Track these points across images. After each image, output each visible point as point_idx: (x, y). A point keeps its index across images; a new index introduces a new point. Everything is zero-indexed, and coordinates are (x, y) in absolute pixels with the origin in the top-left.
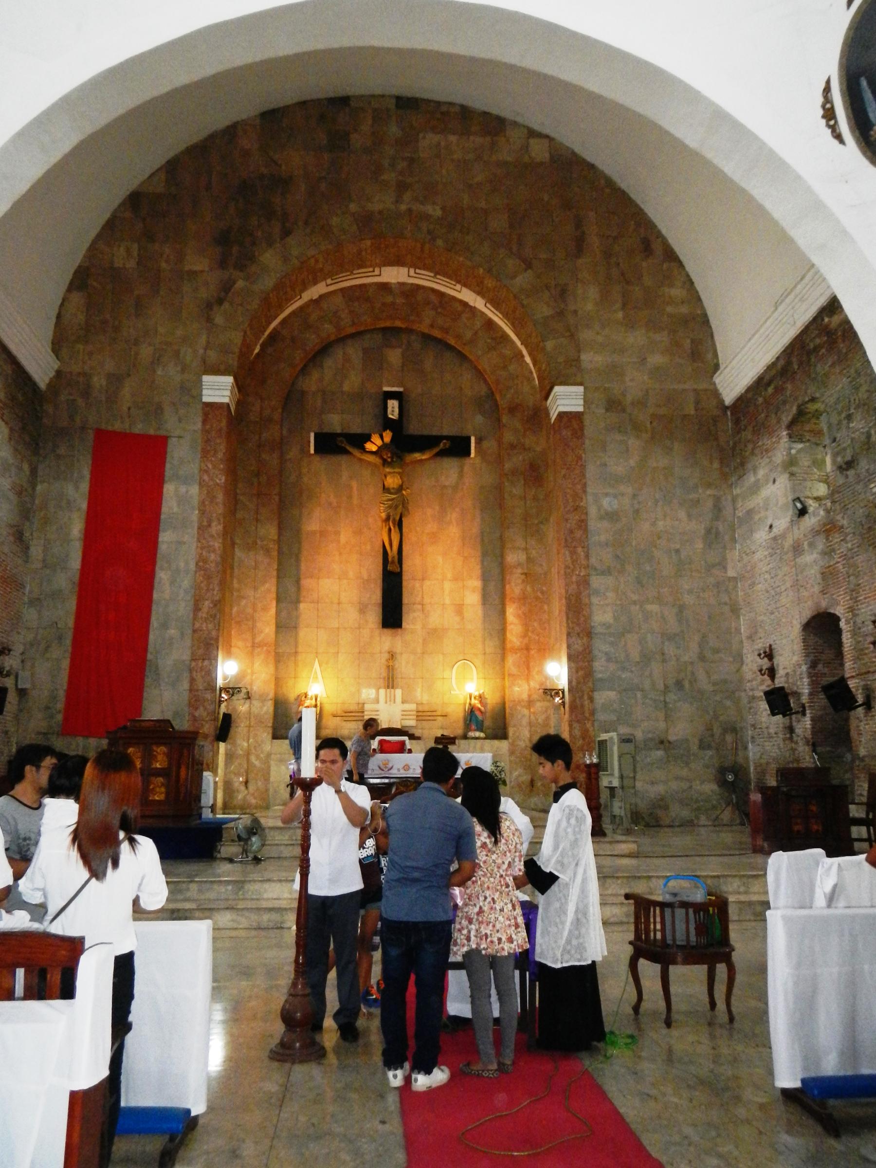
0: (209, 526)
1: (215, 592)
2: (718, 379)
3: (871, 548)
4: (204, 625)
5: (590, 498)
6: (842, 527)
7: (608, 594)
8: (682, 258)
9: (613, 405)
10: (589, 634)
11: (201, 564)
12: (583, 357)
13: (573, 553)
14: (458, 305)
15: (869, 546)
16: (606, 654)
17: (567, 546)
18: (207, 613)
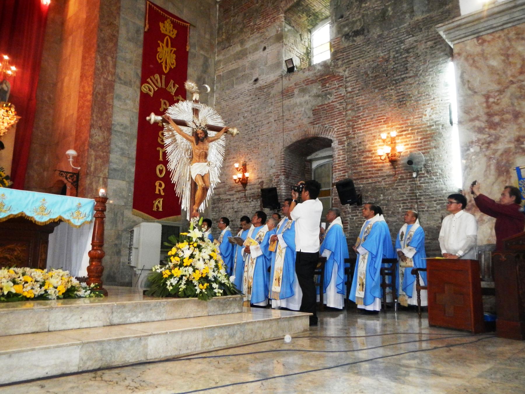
3: (376, 91)
5: (122, 22)
6: (342, 76)
7: (128, 102)
10: (109, 129)
13: (104, 58)
15: (375, 88)
16: (122, 149)
17: (99, 51)
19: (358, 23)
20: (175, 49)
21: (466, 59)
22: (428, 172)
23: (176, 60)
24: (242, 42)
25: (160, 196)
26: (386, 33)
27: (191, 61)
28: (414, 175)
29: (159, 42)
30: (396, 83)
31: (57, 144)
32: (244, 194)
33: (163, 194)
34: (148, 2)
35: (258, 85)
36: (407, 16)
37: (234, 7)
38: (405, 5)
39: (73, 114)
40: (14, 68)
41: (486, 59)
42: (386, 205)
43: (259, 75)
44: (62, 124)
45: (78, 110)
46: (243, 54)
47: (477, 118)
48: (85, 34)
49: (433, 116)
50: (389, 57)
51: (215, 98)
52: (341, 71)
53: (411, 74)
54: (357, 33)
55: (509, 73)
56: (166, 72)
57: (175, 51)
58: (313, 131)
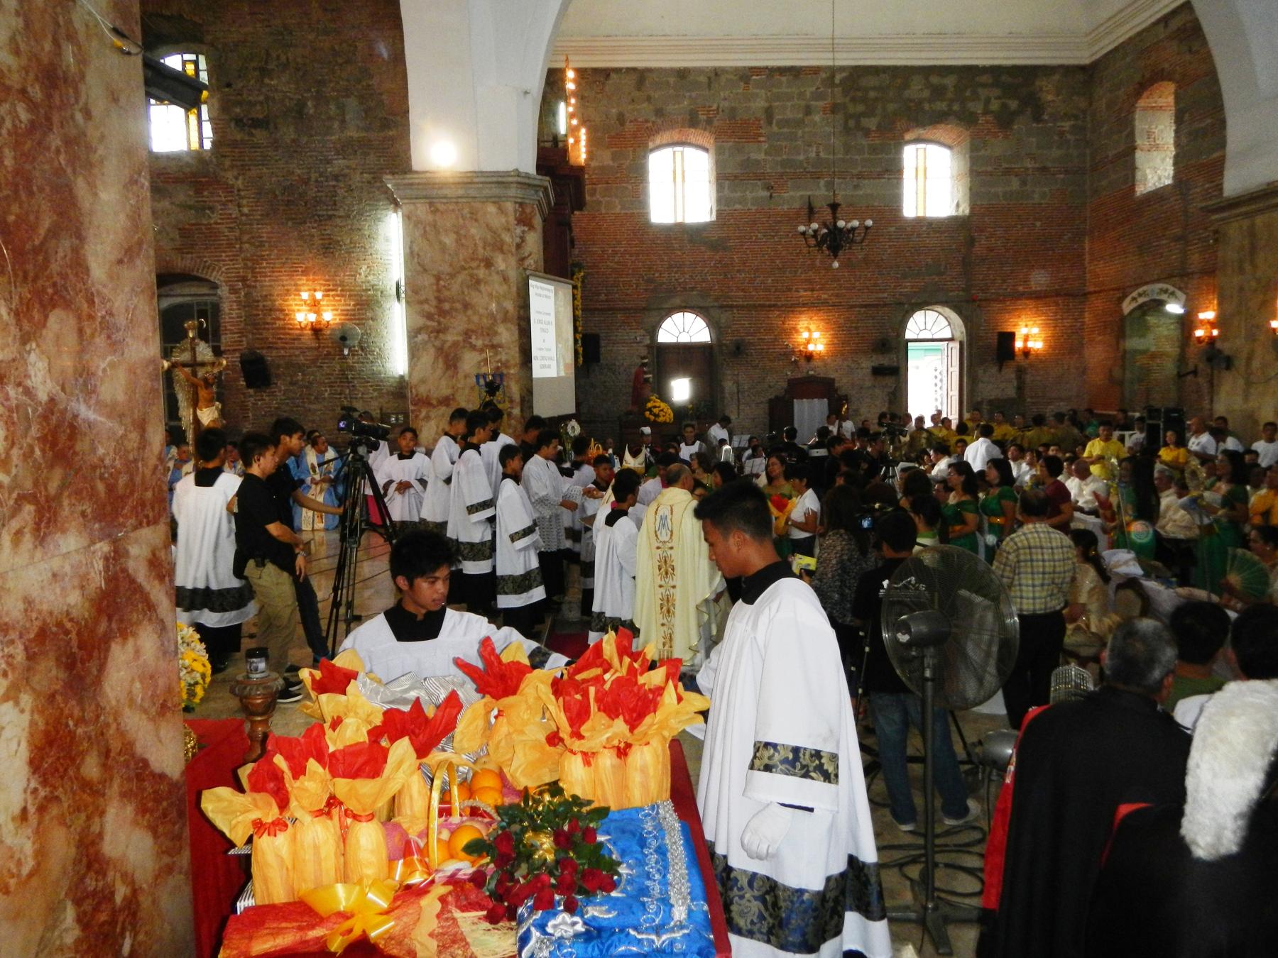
3: (290, 224)
6: (232, 186)
15: (288, 219)
19: (258, 107)
21: (416, 226)
22: (362, 349)
26: (304, 139)
28: (346, 352)
30: (322, 220)
36: (336, 125)
38: (333, 107)
41: (438, 233)
42: (307, 387)
47: (426, 301)
49: (370, 278)
50: (309, 179)
52: (229, 176)
53: (342, 213)
54: (257, 124)
55: (461, 257)
58: (182, 263)
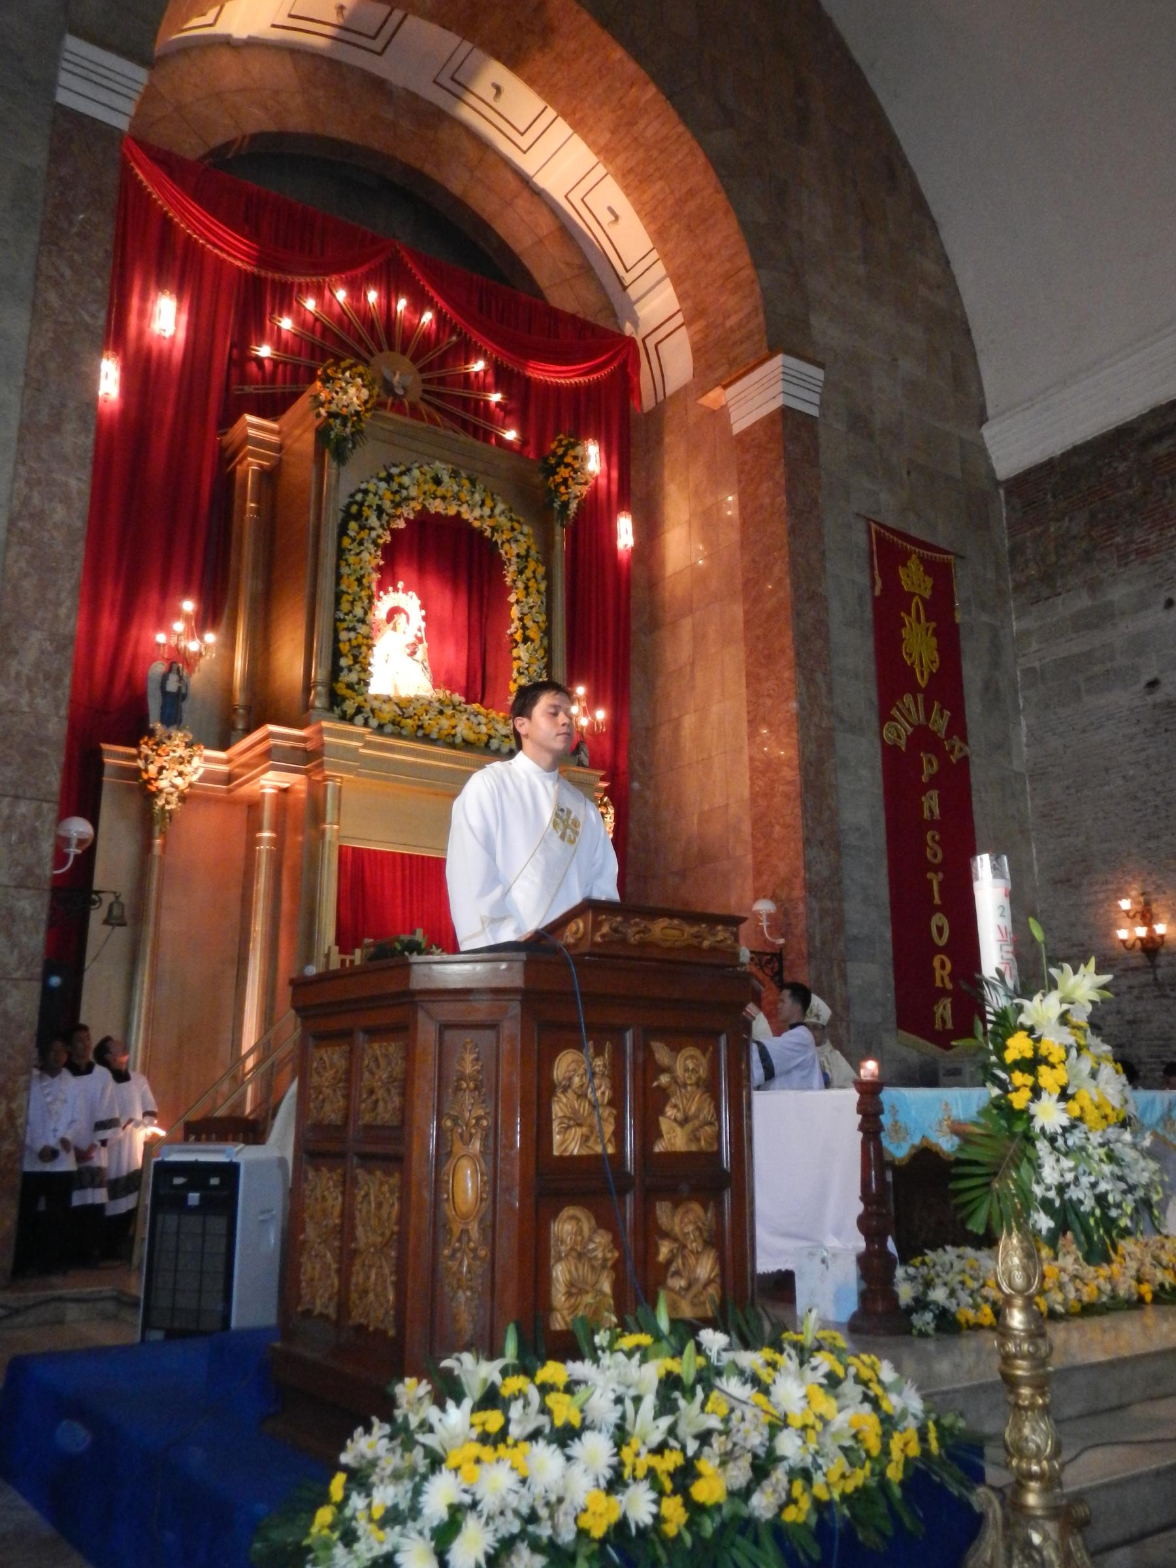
0: (56, 427)
1: (63, 611)
2: (988, 432)
4: (24, 700)
8: (935, 210)
9: (858, 422)
11: (25, 524)
12: (814, 320)
13: (810, 681)
14: (510, 176)
18: (37, 666)
20: (933, 625)
23: (940, 649)
24: (1093, 587)
25: (943, 992)
27: (968, 646)
29: (902, 614)
31: (683, 874)
32: (1151, 977)
33: (949, 986)
34: (873, 525)
35: (1159, 696)
37: (1054, 497)
39: (727, 805)
40: (601, 714)
43: (1161, 672)
44: (692, 823)
45: (754, 799)
46: (1103, 616)
48: (747, 622)
51: (1025, 728)
56: (923, 683)
57: (934, 630)
